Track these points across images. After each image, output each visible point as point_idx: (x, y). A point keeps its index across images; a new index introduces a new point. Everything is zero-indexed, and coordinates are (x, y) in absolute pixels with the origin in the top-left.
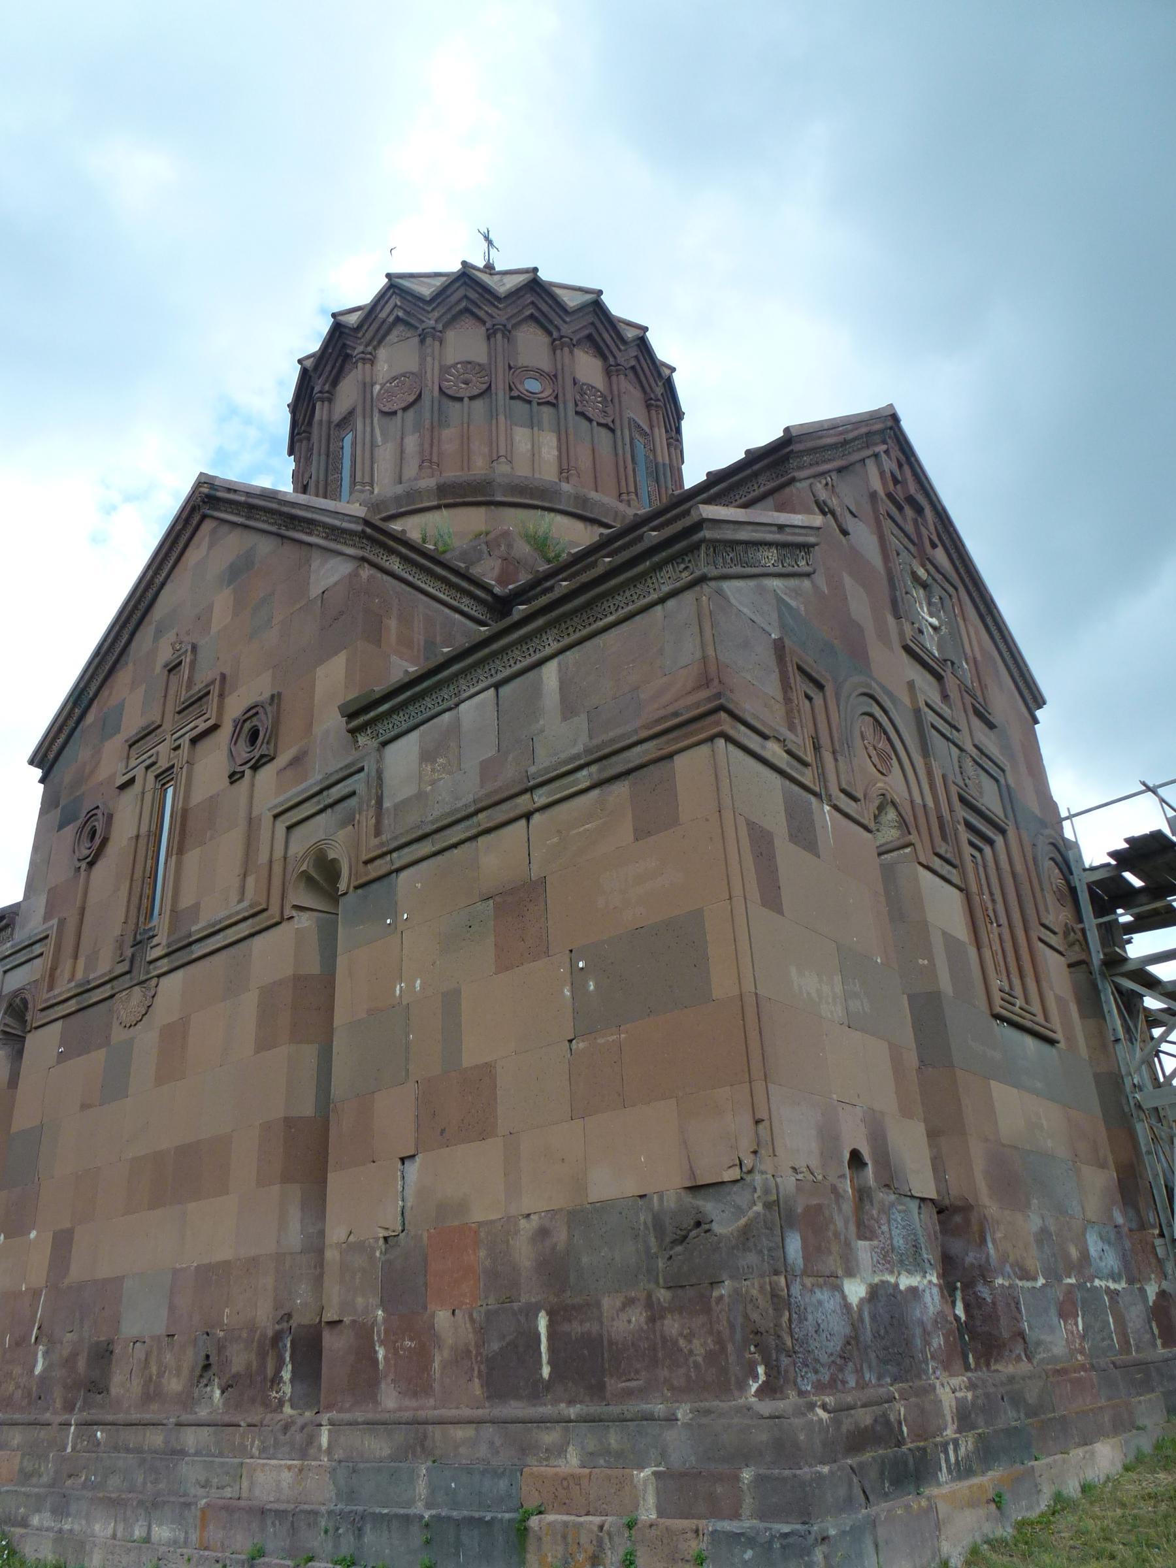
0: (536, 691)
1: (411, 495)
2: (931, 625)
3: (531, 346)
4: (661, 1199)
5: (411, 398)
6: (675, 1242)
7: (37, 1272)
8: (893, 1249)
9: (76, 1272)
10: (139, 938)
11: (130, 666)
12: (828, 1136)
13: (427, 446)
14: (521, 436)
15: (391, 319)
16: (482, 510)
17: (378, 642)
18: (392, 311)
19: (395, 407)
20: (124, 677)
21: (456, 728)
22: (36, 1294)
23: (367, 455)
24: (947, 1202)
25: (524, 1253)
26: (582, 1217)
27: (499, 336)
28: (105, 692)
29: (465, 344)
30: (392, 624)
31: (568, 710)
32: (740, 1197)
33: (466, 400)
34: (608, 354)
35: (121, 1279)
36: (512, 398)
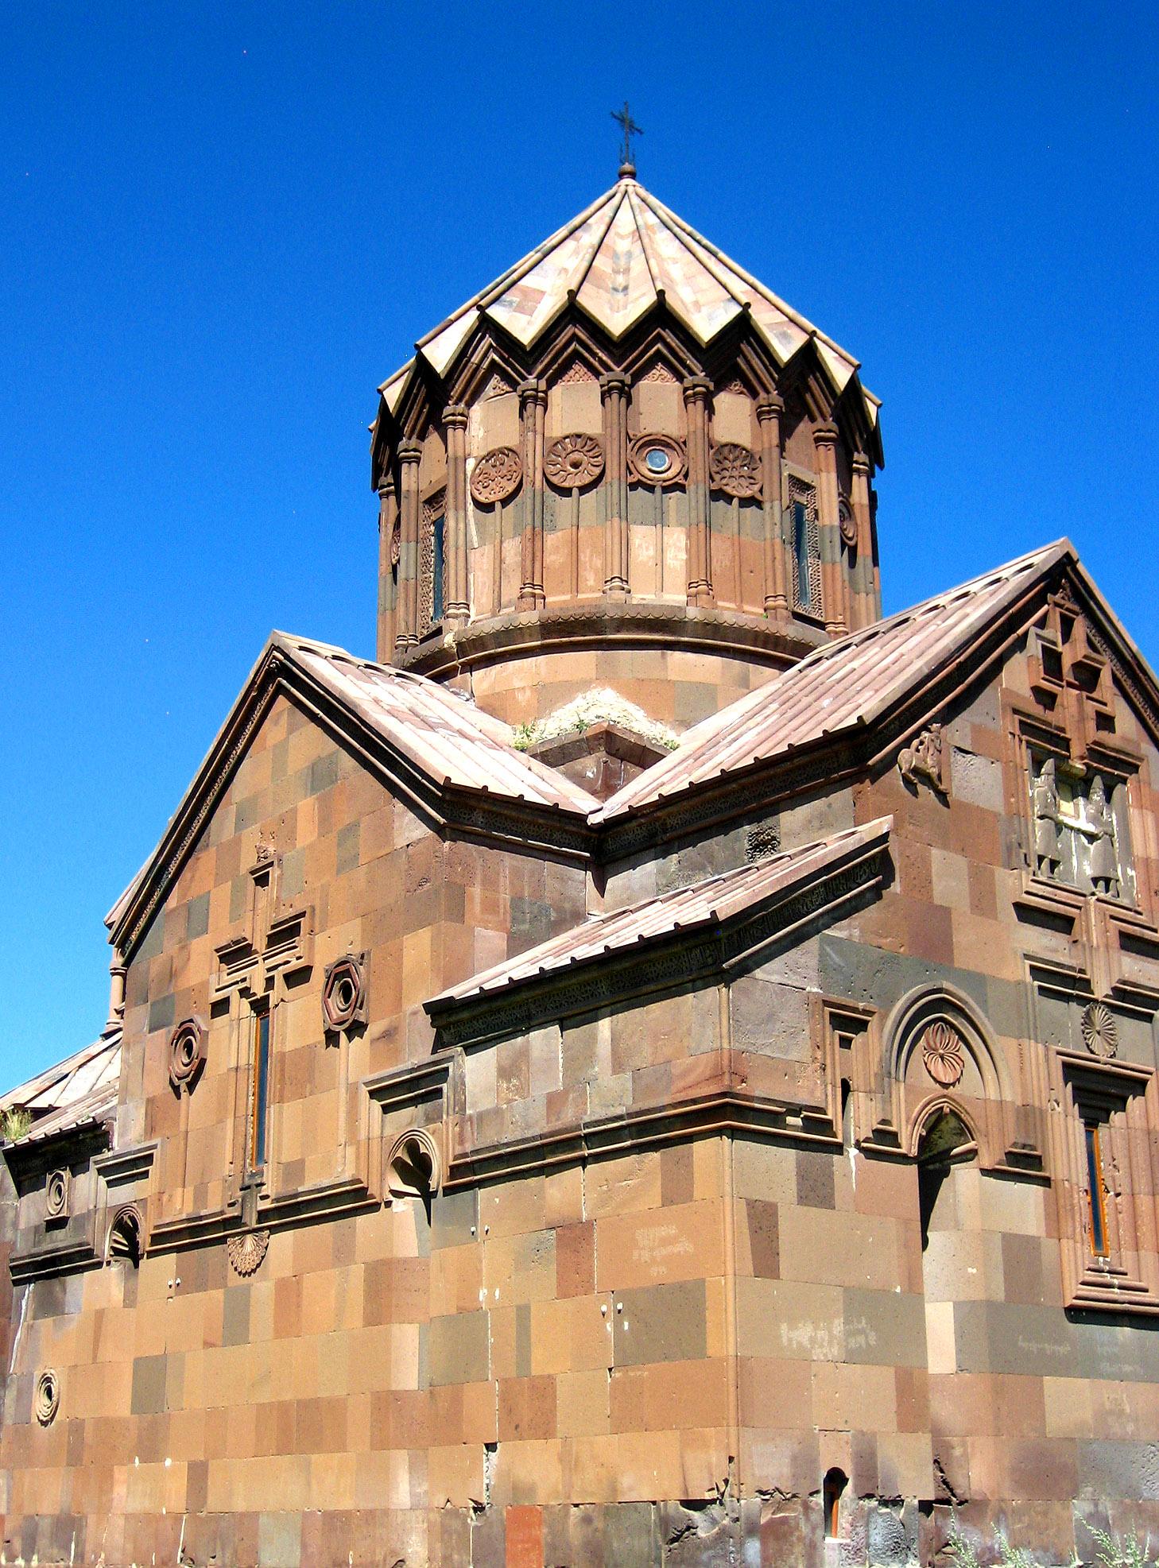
0: (593, 1039)
1: (509, 634)
2: (1085, 833)
3: (660, 399)
4: (665, 1506)
5: (511, 487)
6: (673, 1540)
7: (175, 1495)
8: (868, 1546)
9: (214, 1503)
10: (247, 1182)
11: (213, 849)
12: (804, 1460)
13: (528, 563)
14: (642, 538)
15: (485, 365)
16: (591, 656)
17: (461, 918)
18: (485, 355)
19: (492, 498)
20: (205, 862)
21: (524, 1053)
22: (177, 1518)
23: (461, 564)
24: (967, 1497)
25: (575, 1533)
26: (616, 1510)
27: (615, 396)
28: (186, 874)
29: (576, 404)
30: (476, 891)
31: (618, 1066)
32: (715, 1510)
33: (575, 492)
34: (759, 388)
35: (256, 1514)
36: (633, 486)
